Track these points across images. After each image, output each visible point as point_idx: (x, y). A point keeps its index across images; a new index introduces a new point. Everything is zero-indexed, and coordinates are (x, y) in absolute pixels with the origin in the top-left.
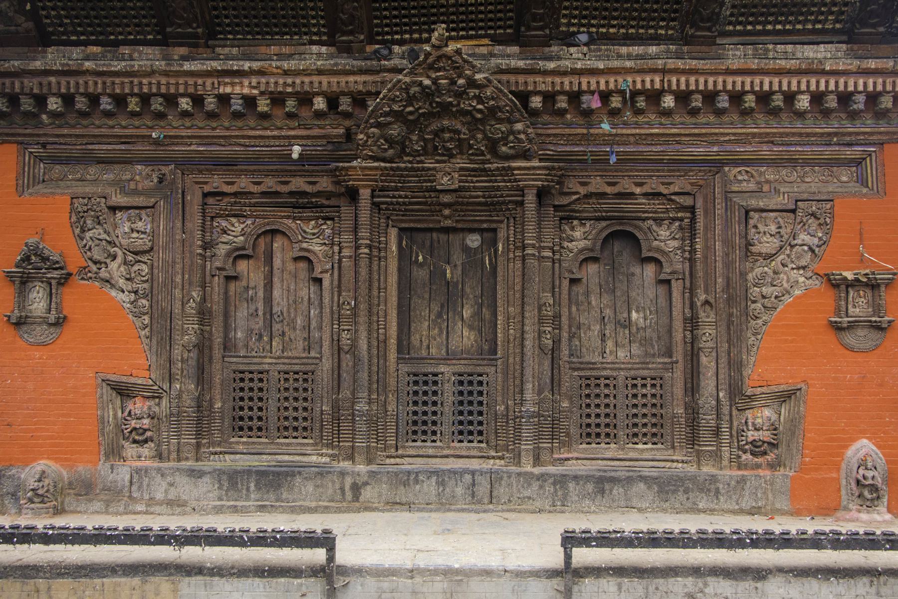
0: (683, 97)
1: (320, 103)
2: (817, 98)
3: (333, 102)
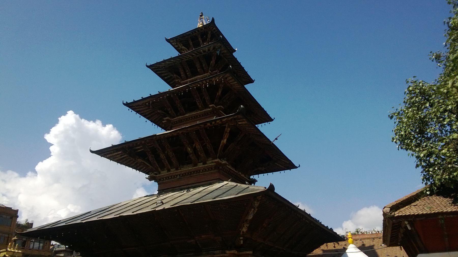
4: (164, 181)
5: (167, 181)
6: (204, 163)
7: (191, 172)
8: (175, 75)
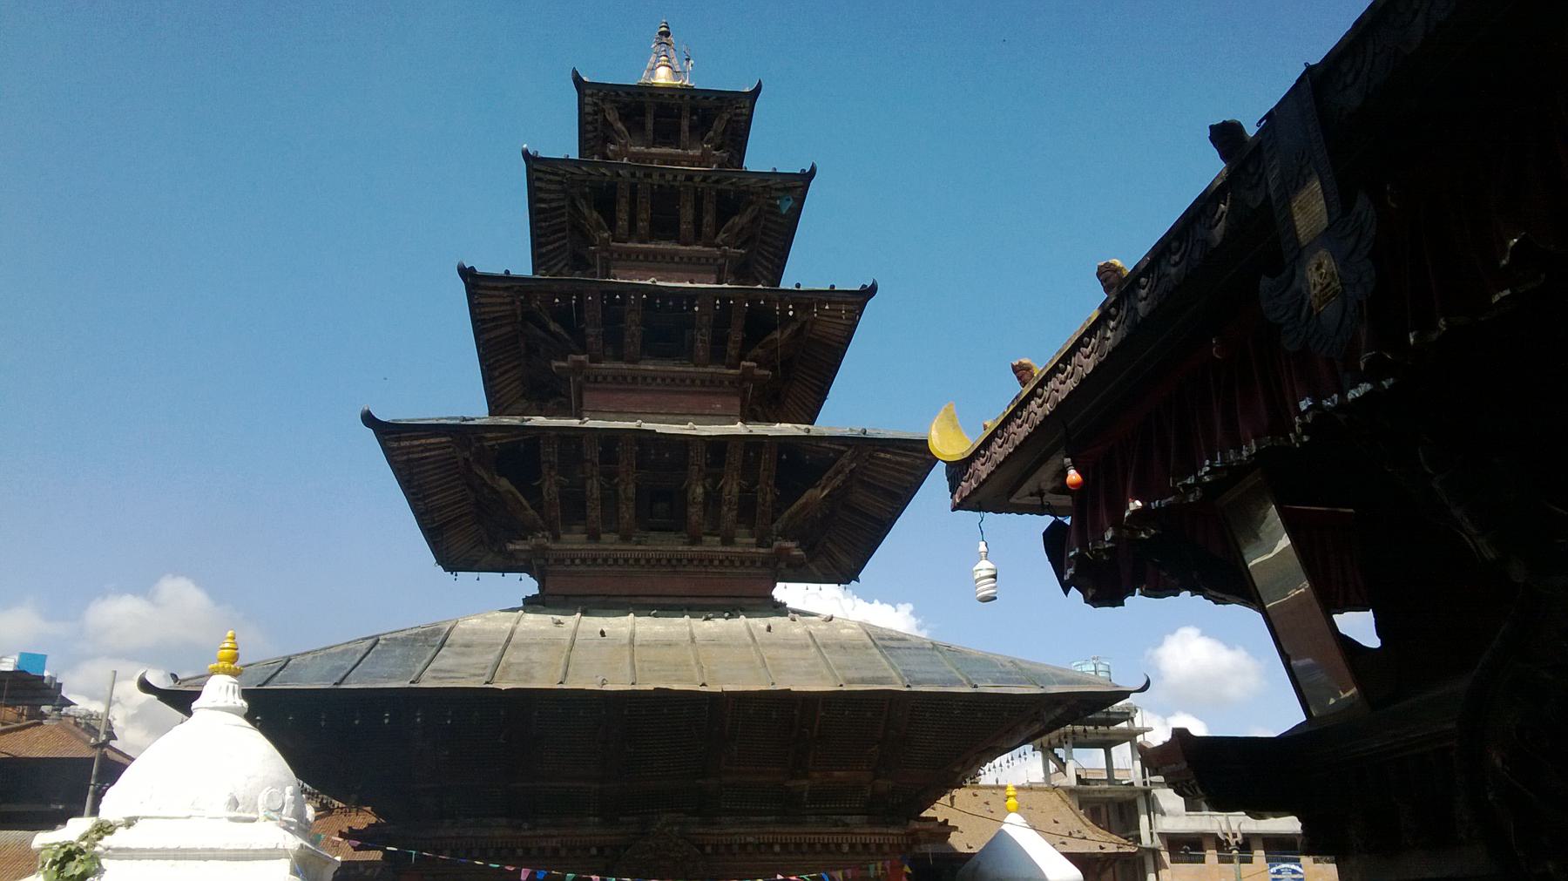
0: (784, 846)
1: (594, 851)
2: (852, 846)
3: (601, 850)
4: (573, 568)
5: (582, 568)
6: (728, 540)
7: (680, 560)
8: (595, 214)
